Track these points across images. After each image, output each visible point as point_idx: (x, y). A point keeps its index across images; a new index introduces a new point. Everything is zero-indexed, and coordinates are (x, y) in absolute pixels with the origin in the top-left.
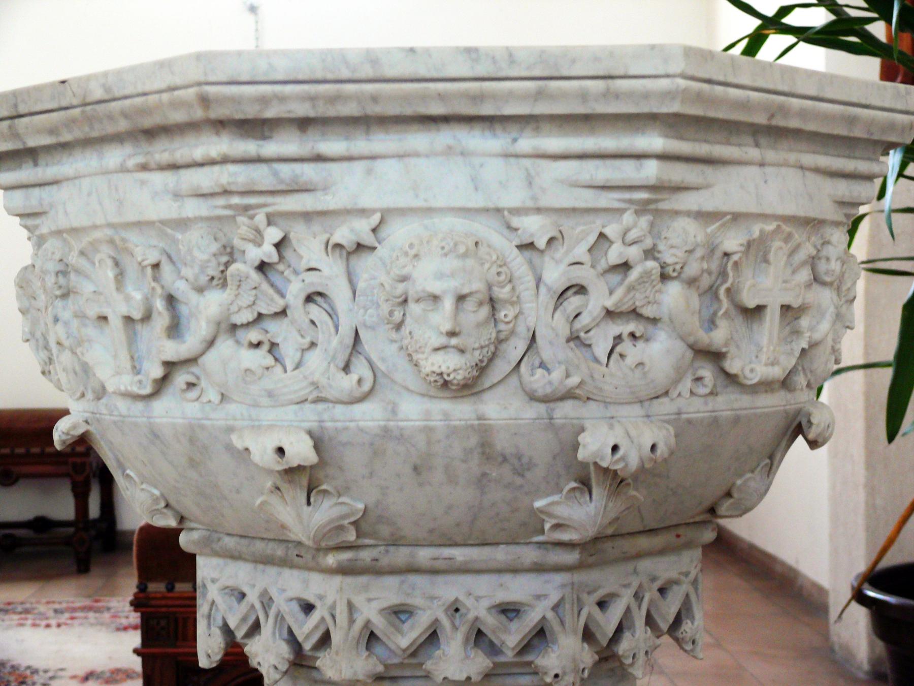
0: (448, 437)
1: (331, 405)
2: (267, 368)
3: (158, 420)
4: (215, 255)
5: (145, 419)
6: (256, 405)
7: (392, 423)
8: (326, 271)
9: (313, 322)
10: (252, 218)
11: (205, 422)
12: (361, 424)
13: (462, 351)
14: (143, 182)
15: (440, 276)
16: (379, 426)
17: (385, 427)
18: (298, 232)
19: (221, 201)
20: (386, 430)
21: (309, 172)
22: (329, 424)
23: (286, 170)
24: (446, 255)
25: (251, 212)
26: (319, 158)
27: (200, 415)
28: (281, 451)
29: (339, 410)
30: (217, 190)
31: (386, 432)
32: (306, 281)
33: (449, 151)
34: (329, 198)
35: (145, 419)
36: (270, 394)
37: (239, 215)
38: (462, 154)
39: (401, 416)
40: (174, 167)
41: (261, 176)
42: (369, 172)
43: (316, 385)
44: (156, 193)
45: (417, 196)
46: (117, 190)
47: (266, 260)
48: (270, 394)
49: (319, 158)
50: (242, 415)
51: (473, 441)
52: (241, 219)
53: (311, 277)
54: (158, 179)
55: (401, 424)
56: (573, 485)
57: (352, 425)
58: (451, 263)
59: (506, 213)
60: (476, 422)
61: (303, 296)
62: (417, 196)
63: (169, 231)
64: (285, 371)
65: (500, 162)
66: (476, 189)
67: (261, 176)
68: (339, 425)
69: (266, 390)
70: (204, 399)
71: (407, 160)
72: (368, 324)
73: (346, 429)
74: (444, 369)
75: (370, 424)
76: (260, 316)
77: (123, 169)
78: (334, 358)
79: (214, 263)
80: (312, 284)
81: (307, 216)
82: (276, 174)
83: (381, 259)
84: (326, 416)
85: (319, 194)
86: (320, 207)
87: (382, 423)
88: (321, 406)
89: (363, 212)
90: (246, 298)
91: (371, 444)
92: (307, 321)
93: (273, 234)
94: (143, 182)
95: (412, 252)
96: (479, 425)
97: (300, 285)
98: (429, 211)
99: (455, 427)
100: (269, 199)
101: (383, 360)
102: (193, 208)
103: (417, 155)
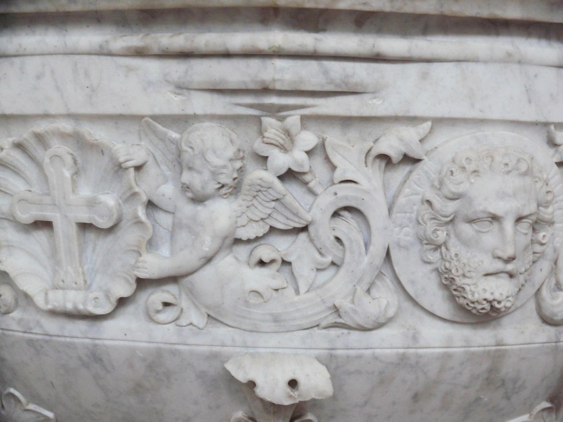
0: (462, 364)
1: (345, 331)
2: (277, 290)
4: (231, 160)
5: (87, 341)
7: (411, 351)
8: (364, 183)
9: (338, 239)
10: (282, 119)
12: (378, 351)
13: (511, 276)
14: (129, 69)
15: (502, 195)
16: (397, 354)
17: (404, 354)
18: (333, 137)
19: (249, 100)
20: (403, 358)
21: (360, 72)
22: (339, 352)
23: (337, 68)
24: (509, 172)
26: (377, 58)
27: (174, 339)
28: (293, 384)
29: (355, 335)
30: (251, 86)
31: (403, 361)
32: (340, 194)
33: (508, 59)
34: (377, 102)
37: (266, 116)
38: (520, 62)
39: (422, 343)
40: (185, 55)
41: (309, 74)
42: (424, 76)
43: (336, 310)
44: (150, 83)
45: (472, 105)
47: (295, 169)
48: (276, 319)
49: (377, 58)
50: (233, 340)
51: (485, 365)
52: (269, 121)
53: (346, 191)
54: (153, 68)
55: (420, 351)
56: (548, 405)
57: (368, 352)
58: (513, 182)
59: (552, 127)
60: (494, 348)
62: (472, 105)
63: (160, 127)
64: (297, 292)
65: (553, 72)
66: (530, 102)
67: (309, 74)
68: (352, 352)
69: (271, 315)
70: (183, 321)
71: (464, 65)
72: (402, 243)
73: (360, 357)
74: (497, 296)
75: (388, 351)
76: (272, 229)
77: (104, 52)
78: (360, 281)
80: (346, 198)
81: (346, 121)
82: (326, 72)
83: (426, 173)
84: (339, 344)
85: (366, 97)
86: (367, 112)
87: (401, 351)
88: (334, 332)
89: (414, 120)
91: (381, 373)
92: (332, 238)
93: (308, 139)
95: (471, 167)
96: (496, 351)
97: (333, 198)
98: (483, 122)
99: (473, 353)
100: (309, 101)
101: (413, 282)
102: (201, 104)
103: (475, 60)
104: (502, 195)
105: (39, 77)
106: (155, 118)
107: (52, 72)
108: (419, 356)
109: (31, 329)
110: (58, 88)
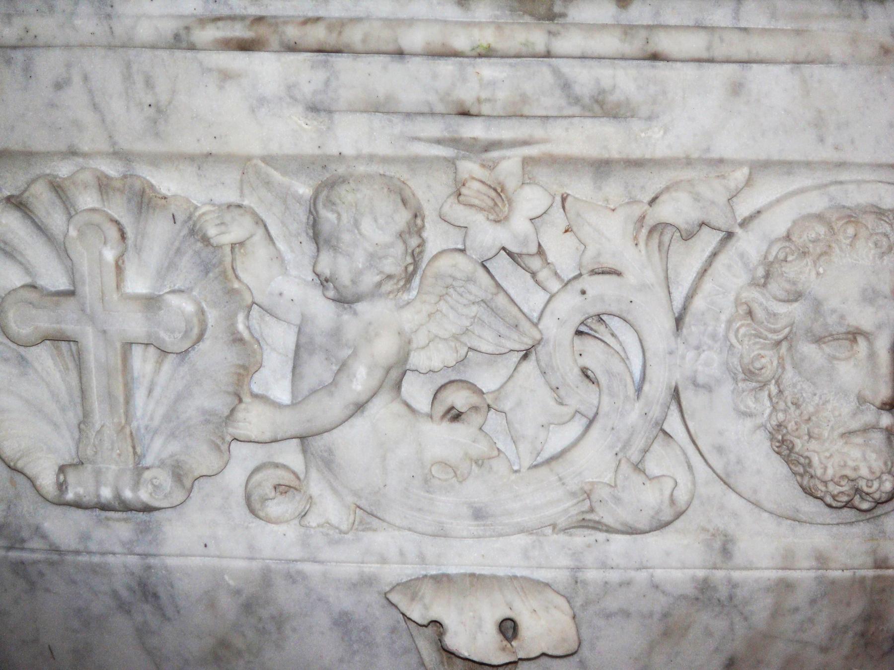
0: (813, 602)
1: (601, 536)
3: (171, 562)
5: (132, 560)
6: (441, 534)
7: (720, 574)
11: (308, 568)
12: (659, 574)
14: (226, 76)
16: (694, 579)
17: (705, 580)
19: (434, 128)
20: (705, 587)
25: (494, 154)
27: (296, 552)
31: (704, 594)
32: (590, 293)
34: (656, 133)
35: (132, 560)
36: (479, 514)
37: (464, 158)
39: (739, 558)
42: (736, 89)
44: (262, 101)
45: (822, 140)
46: (149, 83)
48: (479, 514)
50: (402, 554)
51: (857, 608)
52: (470, 167)
55: (737, 575)
57: (643, 575)
60: (871, 573)
61: (574, 323)
62: (822, 140)
68: (614, 576)
69: (470, 505)
70: (313, 520)
72: (701, 380)
73: (626, 584)
75: (677, 574)
79: (399, 248)
80: (601, 298)
83: (742, 256)
85: (636, 125)
87: (701, 574)
90: (451, 324)
91: (665, 615)
92: (577, 371)
94: (226, 76)
96: (877, 578)
97: (579, 299)
99: (833, 582)
101: (720, 450)
104: (870, 297)
105: (59, 86)
106: (268, 160)
107: (86, 78)
108: (734, 585)
109: (23, 541)
110: (95, 107)
